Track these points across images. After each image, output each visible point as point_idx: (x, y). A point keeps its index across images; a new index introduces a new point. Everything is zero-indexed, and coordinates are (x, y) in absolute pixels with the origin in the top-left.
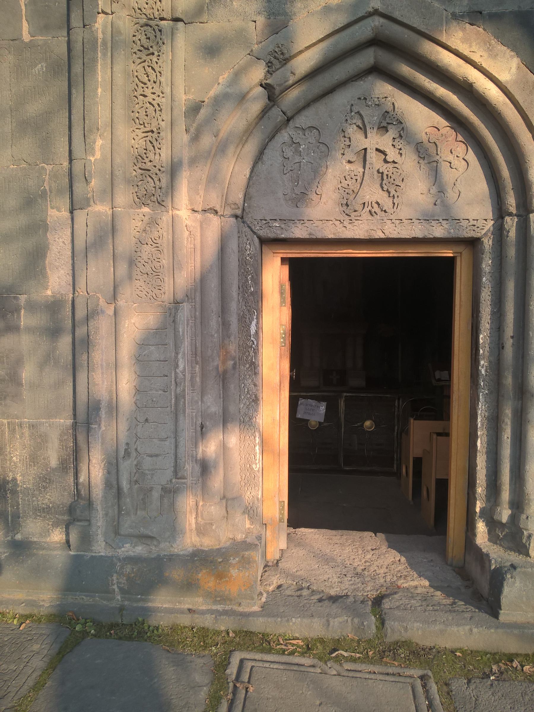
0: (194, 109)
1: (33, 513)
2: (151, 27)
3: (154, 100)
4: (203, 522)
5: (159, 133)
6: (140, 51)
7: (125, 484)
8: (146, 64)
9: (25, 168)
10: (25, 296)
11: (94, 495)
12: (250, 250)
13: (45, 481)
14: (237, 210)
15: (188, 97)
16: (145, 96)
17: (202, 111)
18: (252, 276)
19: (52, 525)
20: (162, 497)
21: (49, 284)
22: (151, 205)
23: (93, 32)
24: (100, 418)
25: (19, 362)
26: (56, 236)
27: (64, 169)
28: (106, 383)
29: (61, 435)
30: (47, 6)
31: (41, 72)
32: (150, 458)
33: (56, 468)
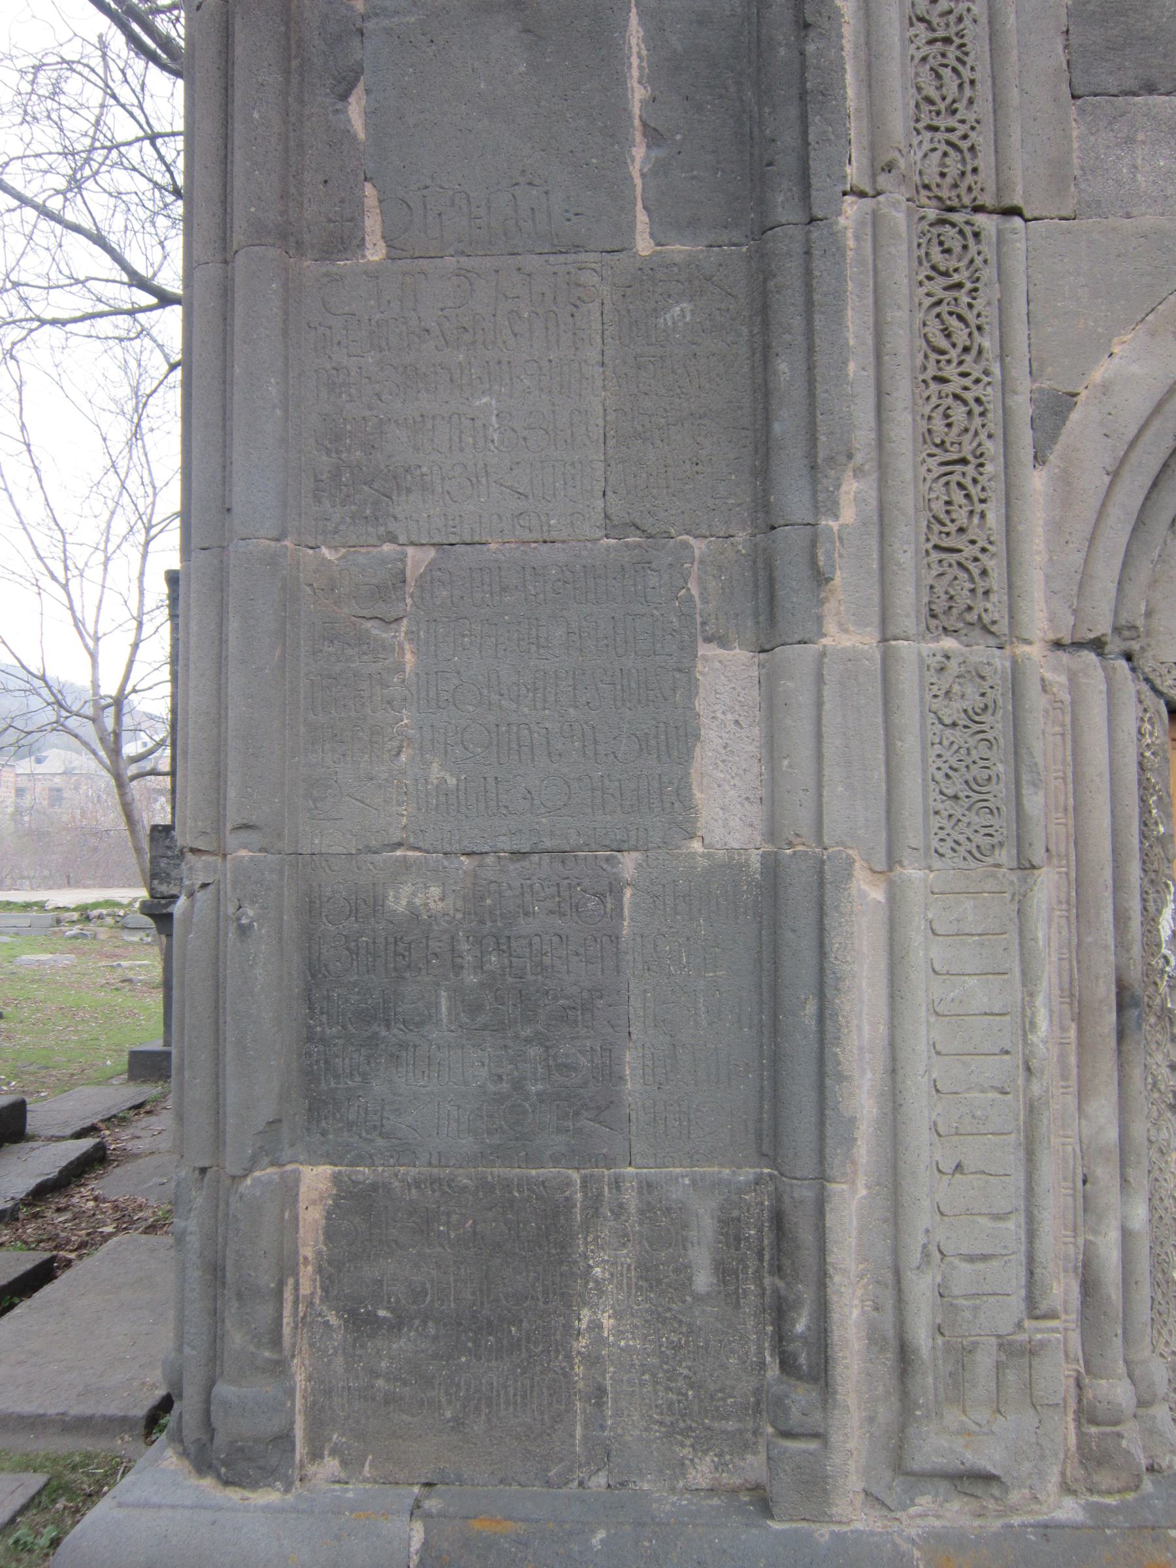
1: (642, 1416)
2: (953, 225)
3: (966, 388)
6: (929, 278)
7: (922, 1336)
8: (944, 309)
9: (639, 545)
12: (1151, 734)
14: (1133, 642)
16: (942, 380)
18: (1160, 798)
19: (692, 1446)
20: (999, 1367)
21: (699, 824)
26: (717, 707)
29: (722, 1209)
30: (694, 178)
31: (680, 324)
32: (966, 1267)
33: (708, 1294)
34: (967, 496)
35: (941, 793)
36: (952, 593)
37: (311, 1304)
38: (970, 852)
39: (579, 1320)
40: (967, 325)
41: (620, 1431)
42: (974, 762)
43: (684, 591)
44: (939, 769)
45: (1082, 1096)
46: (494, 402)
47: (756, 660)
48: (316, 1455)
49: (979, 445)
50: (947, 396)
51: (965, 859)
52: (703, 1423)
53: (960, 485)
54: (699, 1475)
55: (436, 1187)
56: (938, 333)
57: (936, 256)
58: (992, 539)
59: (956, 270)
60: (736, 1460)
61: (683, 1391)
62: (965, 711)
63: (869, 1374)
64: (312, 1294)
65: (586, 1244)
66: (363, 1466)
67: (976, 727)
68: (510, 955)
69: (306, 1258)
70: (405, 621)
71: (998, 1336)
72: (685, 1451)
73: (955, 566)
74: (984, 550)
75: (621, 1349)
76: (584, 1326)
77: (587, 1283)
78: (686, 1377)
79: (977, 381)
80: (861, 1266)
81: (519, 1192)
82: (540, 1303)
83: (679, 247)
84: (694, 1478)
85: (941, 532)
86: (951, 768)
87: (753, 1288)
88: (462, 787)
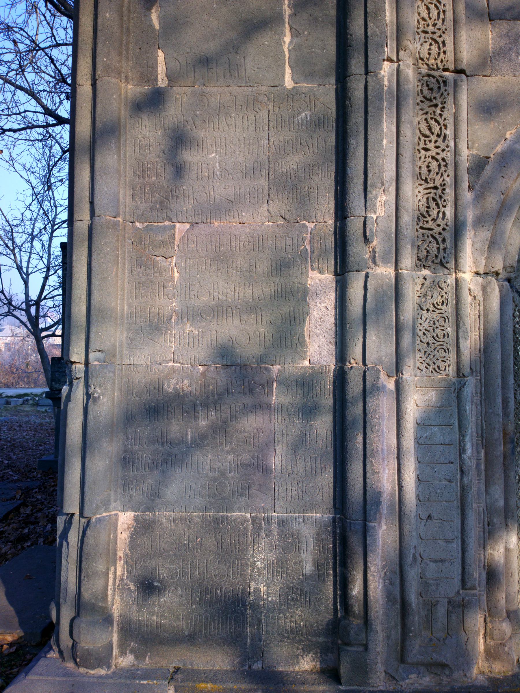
0: (479, 165)
2: (434, 77)
3: (438, 154)
4: (492, 643)
5: (444, 189)
7: (413, 598)
8: (429, 116)
10: (278, 367)
11: (373, 613)
13: (299, 592)
15: (471, 152)
16: (427, 150)
17: (488, 168)
19: (303, 649)
21: (308, 354)
22: (432, 267)
23: (378, 79)
24: (381, 514)
25: (269, 444)
26: (317, 300)
27: (329, 227)
28: (387, 471)
30: (312, 52)
31: (305, 121)
33: (311, 576)
34: (437, 204)
35: (421, 341)
38: (434, 369)
39: (250, 587)
40: (439, 124)
41: (268, 641)
42: (437, 327)
43: (303, 247)
45: (488, 484)
46: (217, 157)
48: (123, 653)
49: (444, 180)
50: (429, 157)
51: (432, 372)
52: (308, 639)
54: (306, 663)
55: (183, 522)
57: (426, 91)
58: (448, 224)
59: (435, 98)
60: (323, 656)
62: (433, 304)
63: (387, 616)
66: (145, 658)
68: (221, 412)
69: (120, 557)
71: (448, 598)
72: (299, 651)
75: (270, 602)
76: (252, 590)
78: (299, 616)
79: (443, 150)
80: (384, 563)
81: (222, 524)
82: (231, 579)
83: (305, 85)
84: (303, 665)
85: (424, 221)
86: (426, 330)
88: (200, 334)
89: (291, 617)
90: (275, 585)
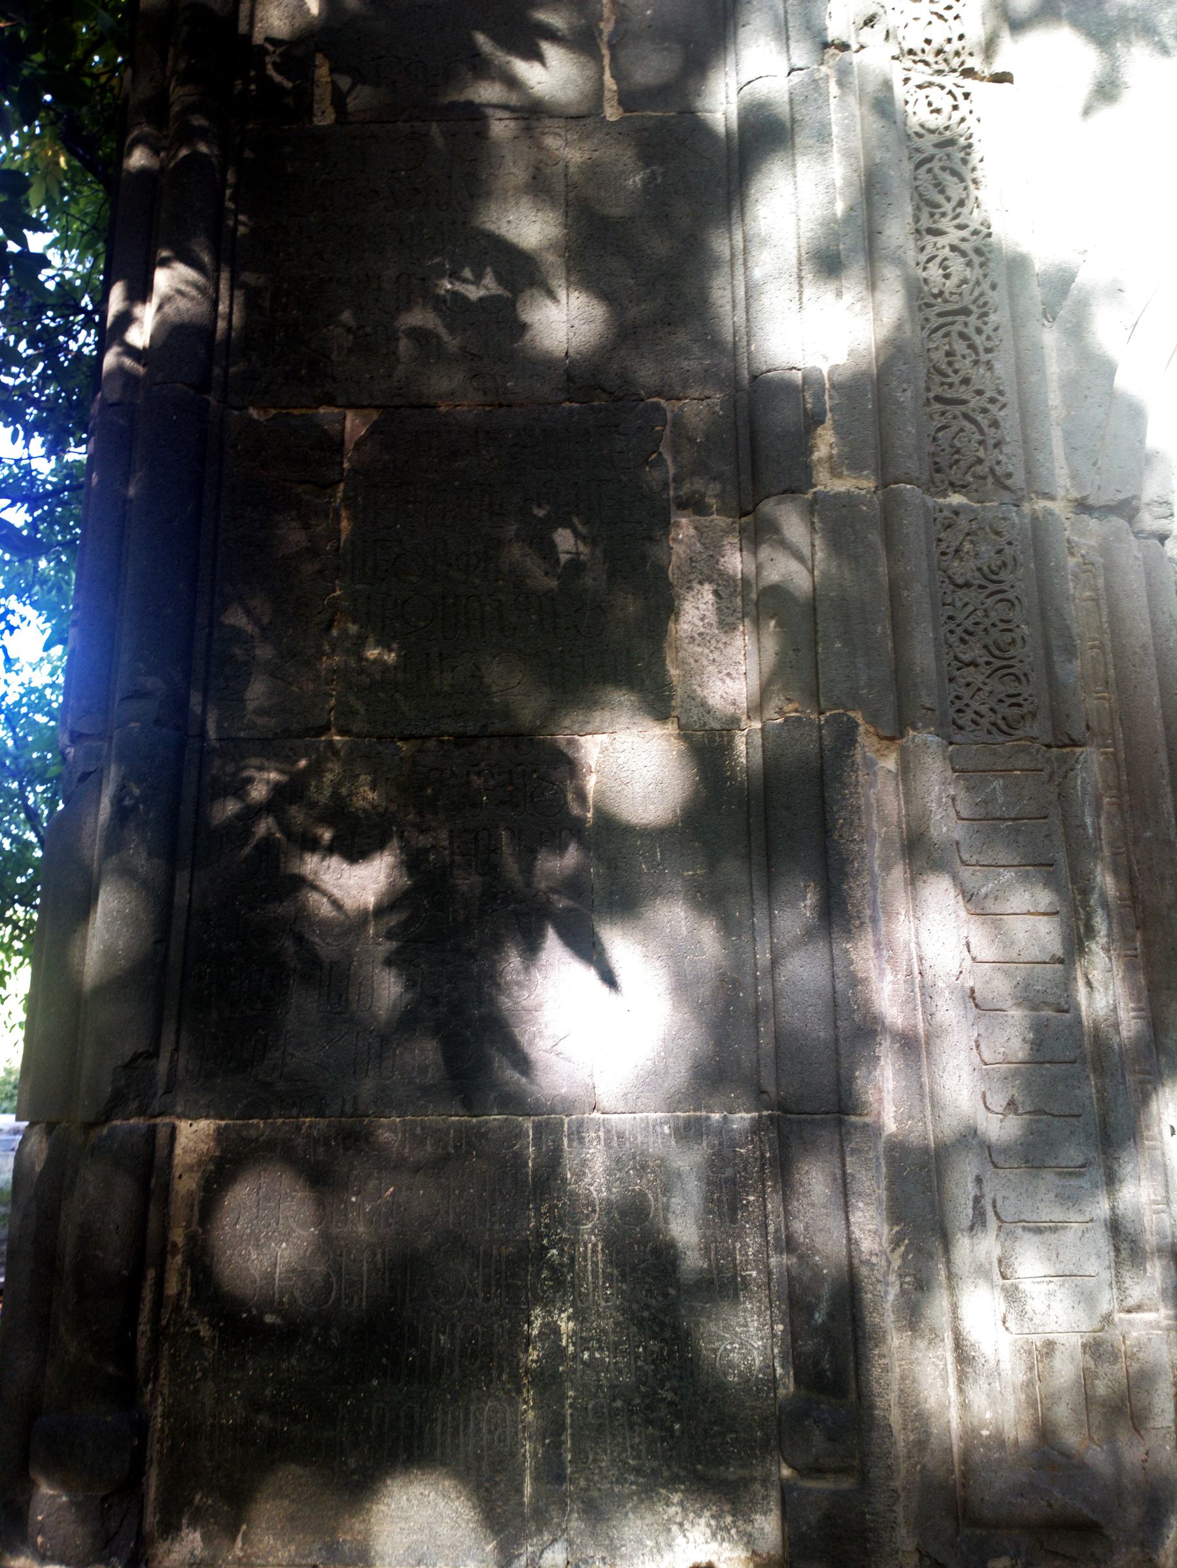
21: (673, 703)
24: (880, 1091)
26: (692, 577)
27: (717, 409)
34: (972, 347)
35: (956, 658)
36: (958, 445)
37: (178, 1308)
38: (994, 724)
39: (530, 1323)
42: (994, 625)
43: (654, 456)
44: (952, 632)
47: (737, 526)
50: (944, 247)
52: (695, 1471)
53: (962, 336)
56: (931, 187)
61: (668, 1424)
62: (979, 569)
64: (179, 1294)
65: (539, 1215)
66: (234, 1540)
67: (993, 587)
69: (175, 1245)
70: (342, 486)
72: (672, 1510)
73: (961, 418)
74: (993, 401)
75: (584, 1363)
76: (535, 1332)
77: (539, 1271)
78: (670, 1404)
80: (896, 1228)
85: (943, 384)
86: (966, 631)
87: (754, 1274)
89: (648, 1407)
90: (599, 1316)
